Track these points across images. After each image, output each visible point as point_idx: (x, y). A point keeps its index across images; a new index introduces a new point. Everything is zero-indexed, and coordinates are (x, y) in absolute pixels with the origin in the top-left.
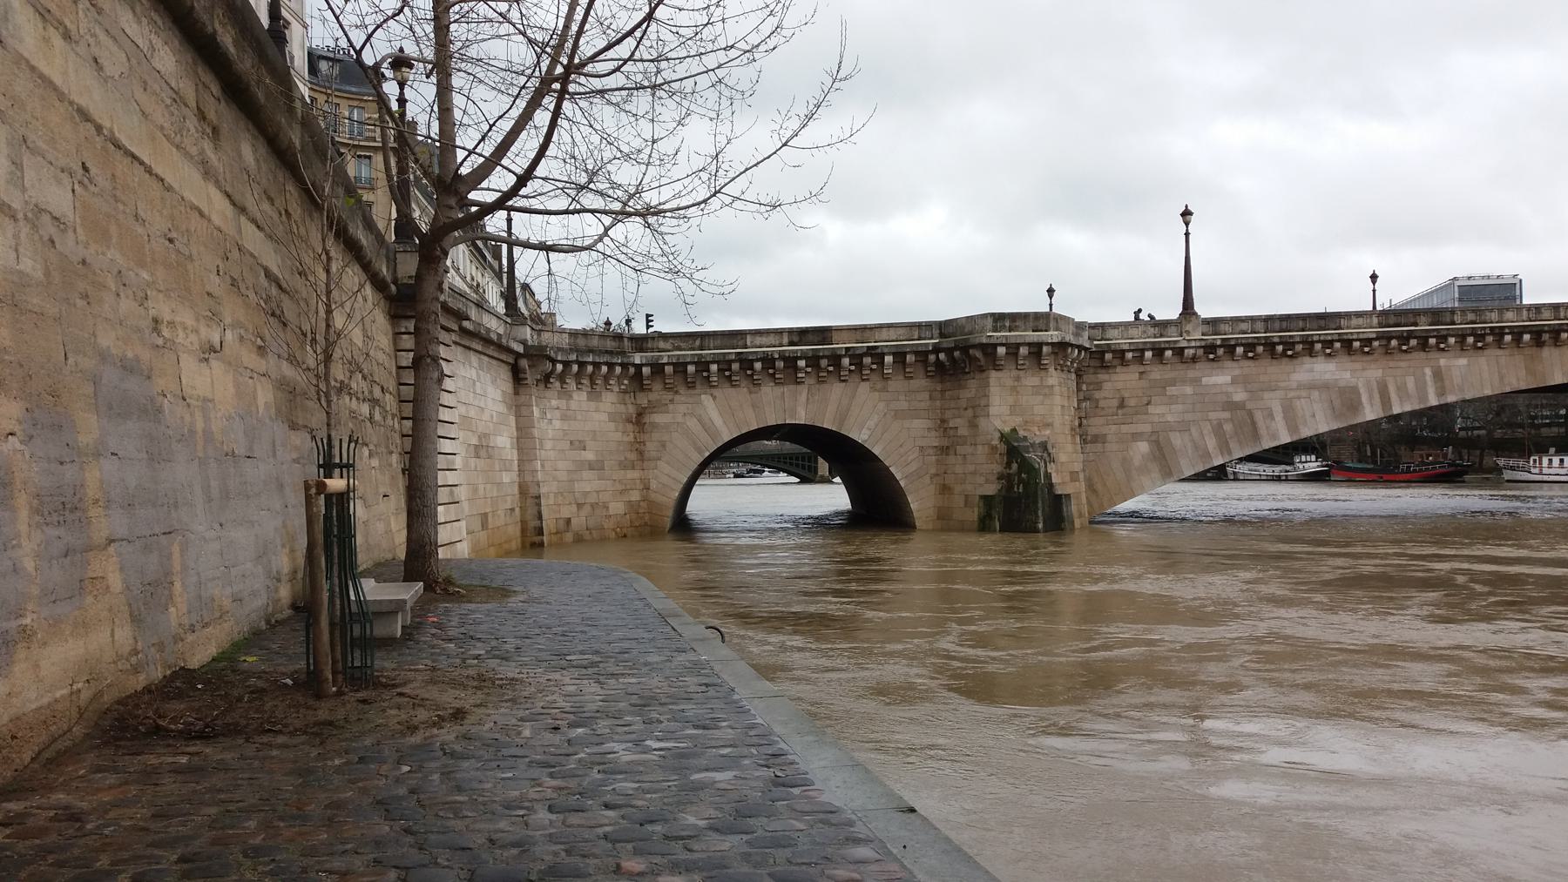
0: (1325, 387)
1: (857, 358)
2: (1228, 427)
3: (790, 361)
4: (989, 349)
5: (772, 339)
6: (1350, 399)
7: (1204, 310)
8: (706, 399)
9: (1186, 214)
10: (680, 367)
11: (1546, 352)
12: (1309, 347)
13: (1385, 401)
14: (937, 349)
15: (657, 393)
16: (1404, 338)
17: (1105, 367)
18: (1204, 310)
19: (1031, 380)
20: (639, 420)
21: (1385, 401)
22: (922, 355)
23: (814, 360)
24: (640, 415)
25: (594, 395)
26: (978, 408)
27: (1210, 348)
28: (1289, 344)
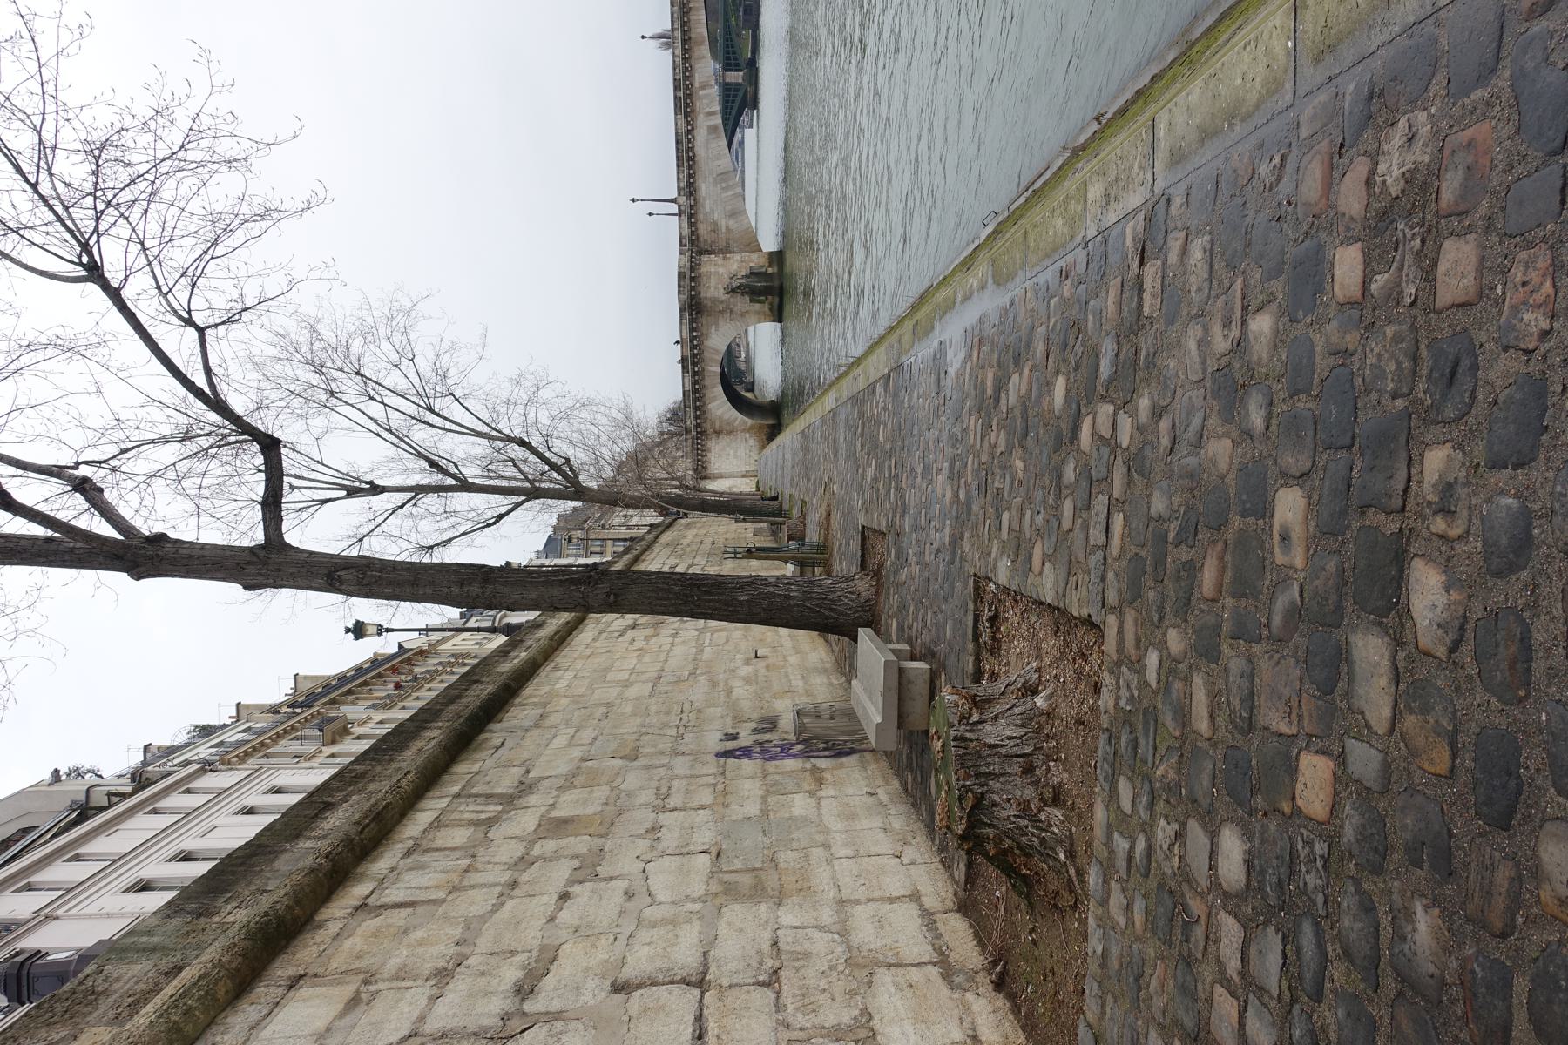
0: (707, 141)
1: (693, 347)
2: (724, 185)
3: (695, 374)
4: (691, 297)
5: (686, 380)
6: (713, 129)
7: (674, 195)
8: (710, 406)
9: (633, 200)
10: (697, 417)
11: (693, 36)
12: (690, 149)
13: (712, 113)
14: (691, 314)
15: (708, 425)
16: (687, 105)
17: (698, 238)
18: (674, 195)
19: (705, 279)
20: (718, 433)
21: (712, 113)
22: (692, 321)
23: (694, 364)
24: (715, 432)
25: (709, 450)
26: (715, 301)
27: (690, 194)
28: (689, 159)
